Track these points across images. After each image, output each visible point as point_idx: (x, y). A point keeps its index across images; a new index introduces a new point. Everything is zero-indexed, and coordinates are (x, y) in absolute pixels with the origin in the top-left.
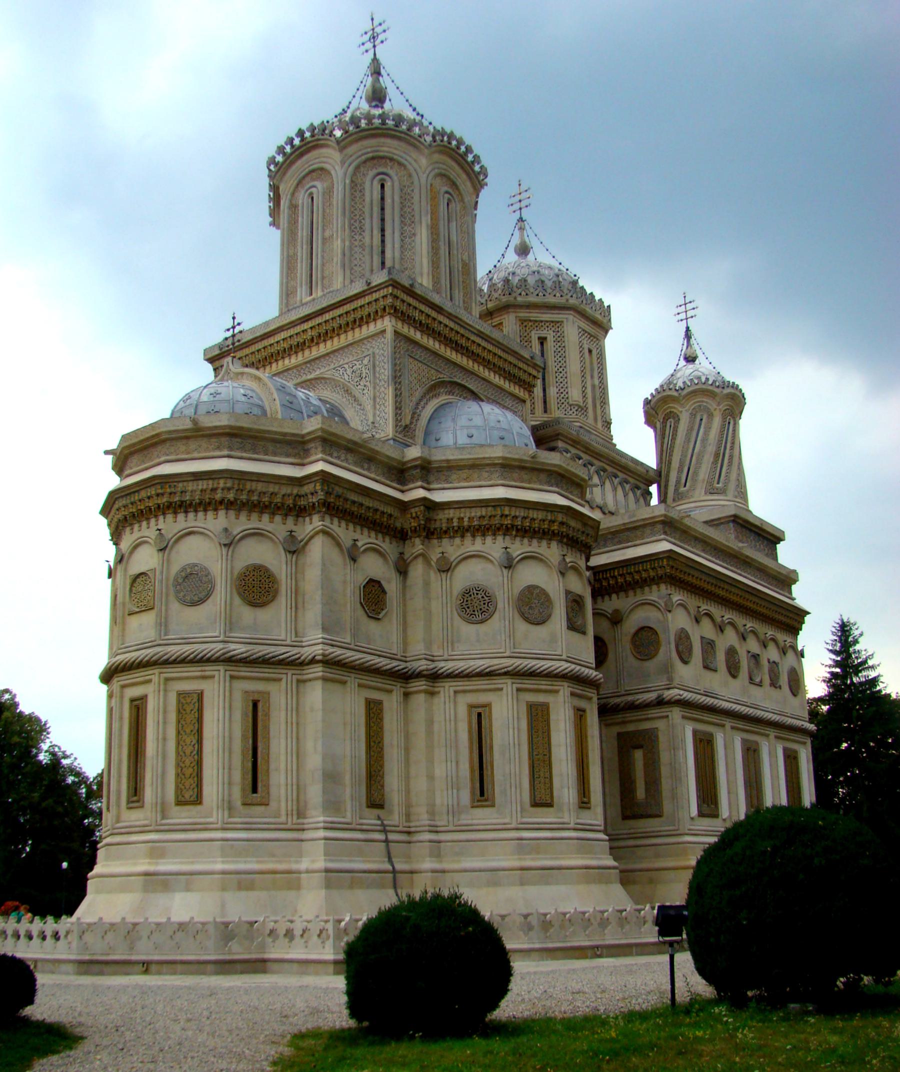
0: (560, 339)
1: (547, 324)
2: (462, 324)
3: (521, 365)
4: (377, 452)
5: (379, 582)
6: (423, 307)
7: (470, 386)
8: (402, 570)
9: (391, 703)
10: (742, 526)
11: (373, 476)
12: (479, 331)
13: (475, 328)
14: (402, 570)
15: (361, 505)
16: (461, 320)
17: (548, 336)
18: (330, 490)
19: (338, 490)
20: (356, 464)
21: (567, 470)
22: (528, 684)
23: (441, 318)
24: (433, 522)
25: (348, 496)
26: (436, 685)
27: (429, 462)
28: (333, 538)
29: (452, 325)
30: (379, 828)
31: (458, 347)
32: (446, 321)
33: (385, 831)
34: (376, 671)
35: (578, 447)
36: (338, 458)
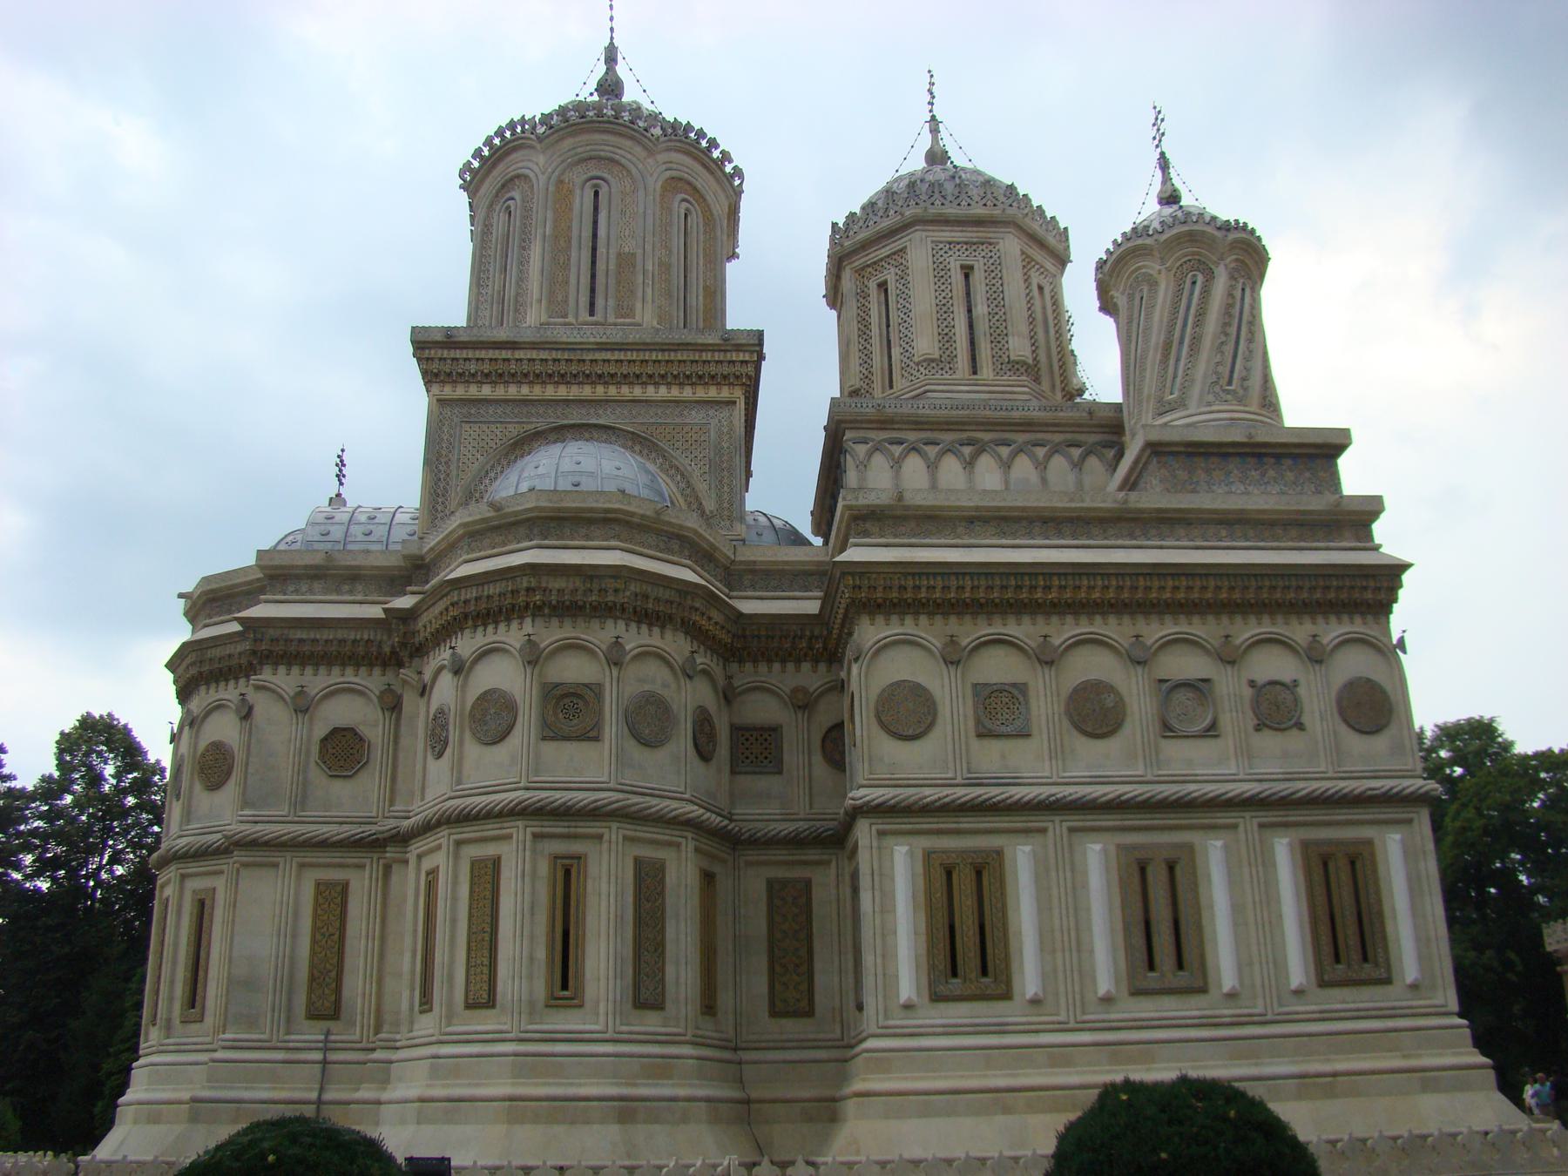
0: (902, 277)
1: (958, 247)
2: (564, 346)
3: (707, 356)
4: (359, 567)
5: (352, 729)
6: (482, 354)
7: (601, 422)
8: (392, 705)
9: (361, 884)
10: (1190, 455)
11: (359, 598)
12: (598, 344)
13: (589, 343)
14: (392, 705)
15: (315, 641)
16: (556, 343)
17: (888, 277)
18: (259, 636)
19: (272, 633)
20: (326, 591)
21: (559, 510)
22: (469, 832)
23: (519, 354)
24: (416, 635)
25: (291, 636)
26: (409, 849)
27: (422, 558)
28: (273, 691)
29: (544, 355)
30: (321, 1045)
31: (563, 379)
32: (534, 354)
33: (326, 1050)
34: (324, 844)
35: (896, 426)
36: (296, 592)
